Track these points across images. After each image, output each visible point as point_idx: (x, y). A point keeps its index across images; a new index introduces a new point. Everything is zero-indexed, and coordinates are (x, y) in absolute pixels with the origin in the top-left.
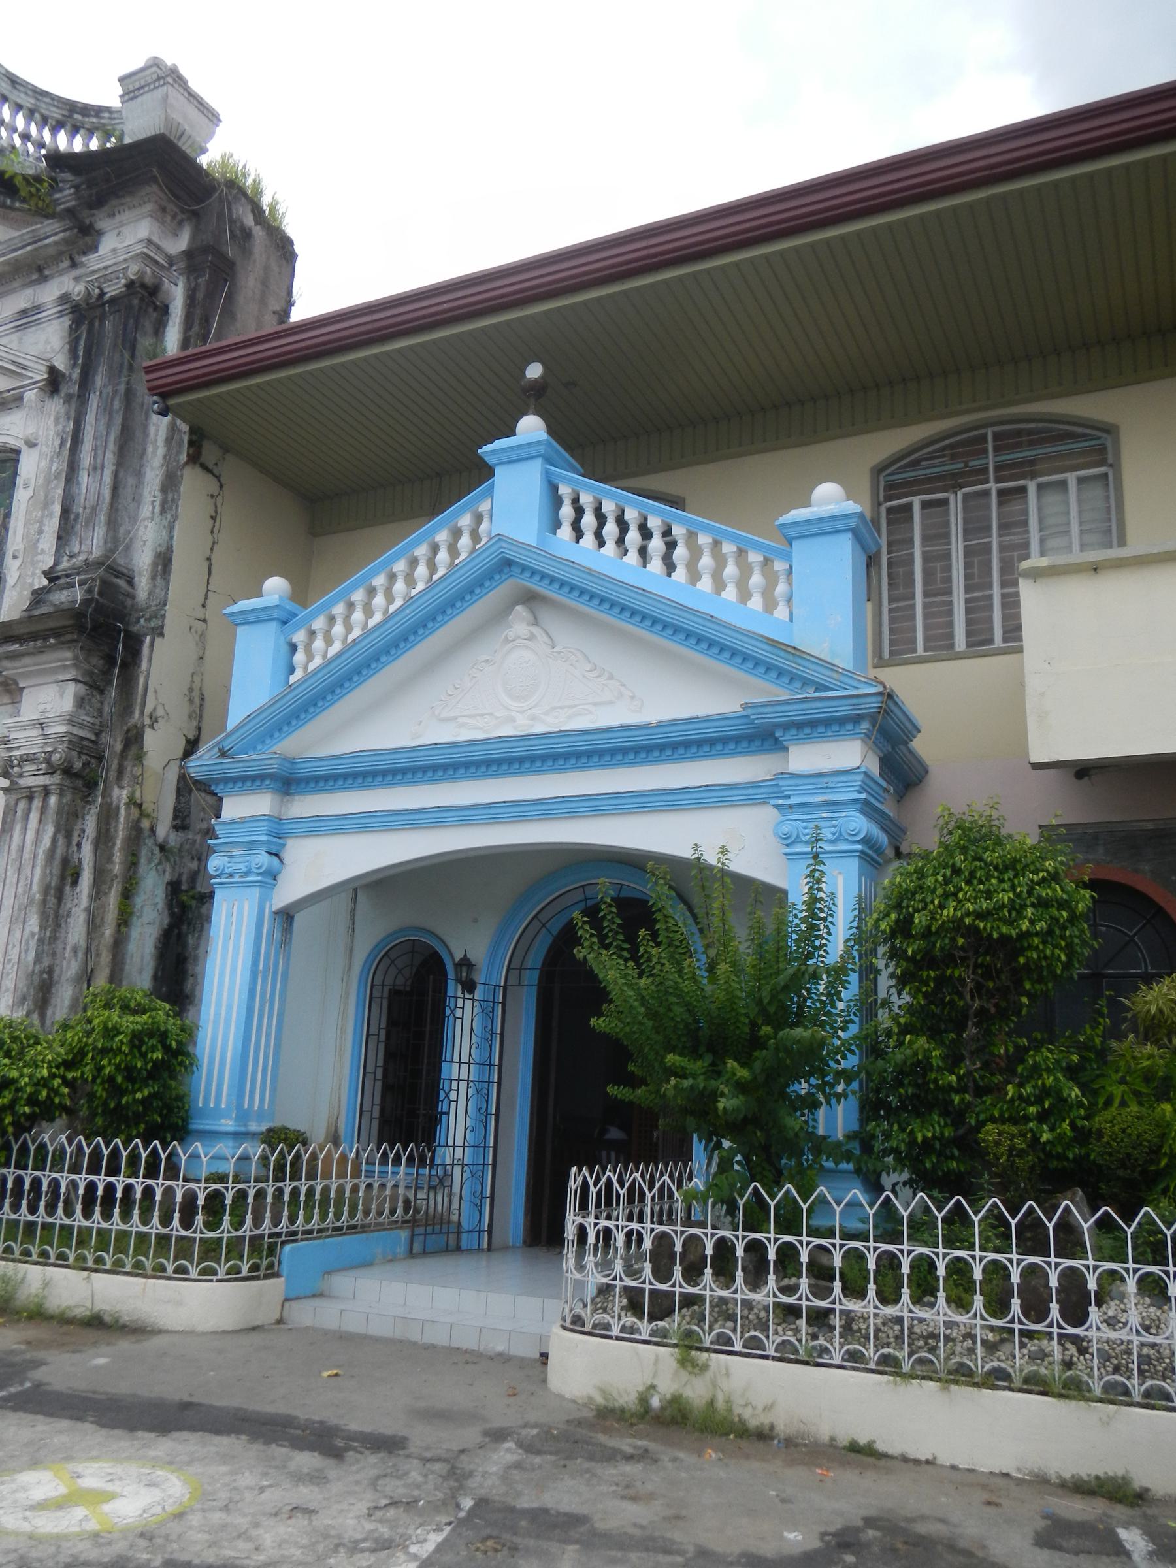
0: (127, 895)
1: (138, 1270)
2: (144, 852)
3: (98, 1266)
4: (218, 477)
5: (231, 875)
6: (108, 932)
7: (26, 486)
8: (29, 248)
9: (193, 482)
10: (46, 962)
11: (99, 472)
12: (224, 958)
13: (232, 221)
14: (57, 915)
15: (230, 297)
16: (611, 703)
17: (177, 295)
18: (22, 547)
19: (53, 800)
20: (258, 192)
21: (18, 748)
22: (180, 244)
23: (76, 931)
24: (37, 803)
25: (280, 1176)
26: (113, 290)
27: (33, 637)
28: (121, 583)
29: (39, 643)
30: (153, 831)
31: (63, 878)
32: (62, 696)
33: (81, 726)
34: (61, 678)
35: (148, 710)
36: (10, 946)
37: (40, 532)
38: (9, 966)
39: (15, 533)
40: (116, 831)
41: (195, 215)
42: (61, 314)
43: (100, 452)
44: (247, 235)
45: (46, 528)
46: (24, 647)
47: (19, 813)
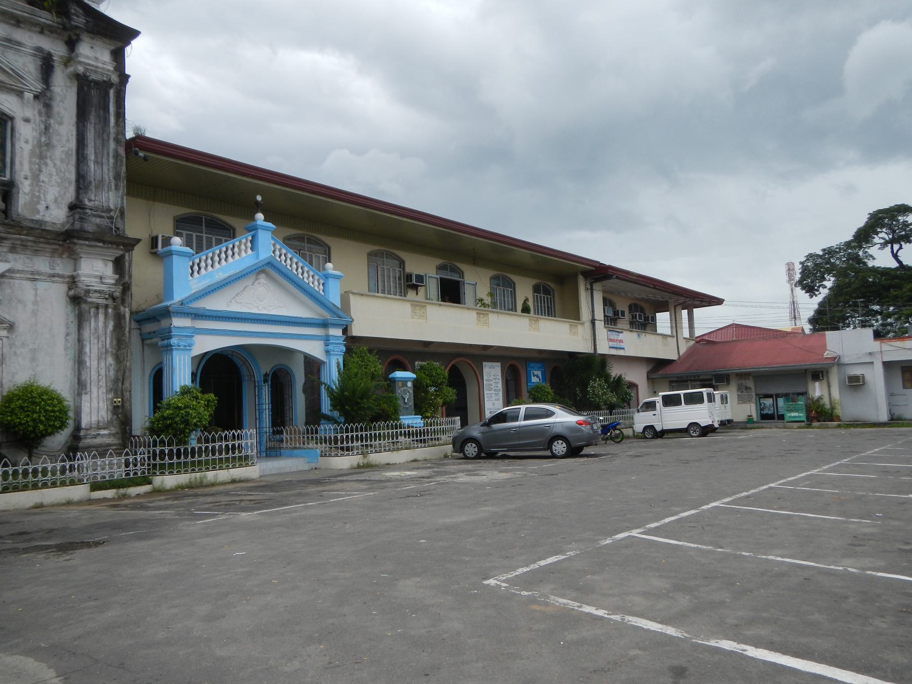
1: (241, 466)
3: (228, 467)
5: (179, 346)
7: (27, 142)
8: (26, 14)
11: (100, 165)
12: (180, 375)
16: (282, 307)
18: (29, 174)
19: (110, 310)
21: (93, 286)
24: (101, 311)
25: (308, 433)
26: (93, 77)
27: (111, 243)
29: (114, 246)
32: (106, 265)
34: (106, 258)
36: (100, 369)
37: (40, 171)
38: (100, 377)
39: (21, 164)
40: (125, 324)
42: (34, 55)
43: (99, 156)
45: (44, 170)
46: (106, 246)
47: (92, 313)
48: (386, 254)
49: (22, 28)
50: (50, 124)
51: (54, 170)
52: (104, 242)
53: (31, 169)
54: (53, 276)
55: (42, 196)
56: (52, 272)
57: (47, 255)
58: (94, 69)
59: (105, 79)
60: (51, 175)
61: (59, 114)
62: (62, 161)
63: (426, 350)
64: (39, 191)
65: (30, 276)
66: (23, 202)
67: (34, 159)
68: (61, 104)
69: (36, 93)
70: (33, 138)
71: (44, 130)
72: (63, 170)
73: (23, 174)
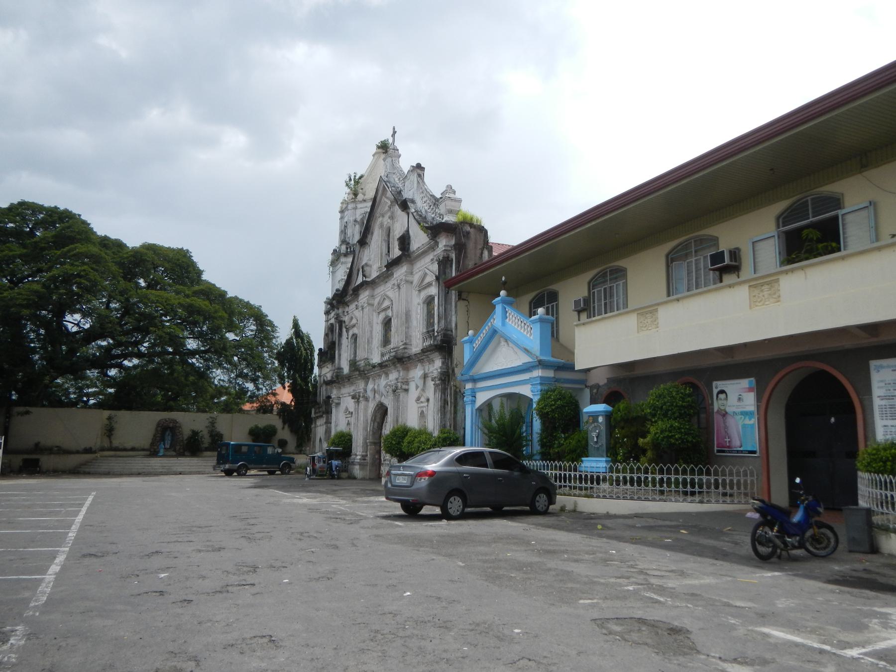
0: (455, 407)
2: (458, 396)
4: (467, 300)
6: (452, 415)
9: (462, 304)
10: (443, 423)
13: (463, 232)
14: (444, 412)
15: (465, 253)
17: (453, 256)
20: (472, 219)
22: (453, 242)
23: (448, 416)
28: (449, 333)
30: (460, 391)
31: (445, 404)
33: (443, 369)
35: (455, 363)
41: (455, 234)
44: (468, 233)
48: (695, 241)
52: (430, 351)
63: (729, 360)
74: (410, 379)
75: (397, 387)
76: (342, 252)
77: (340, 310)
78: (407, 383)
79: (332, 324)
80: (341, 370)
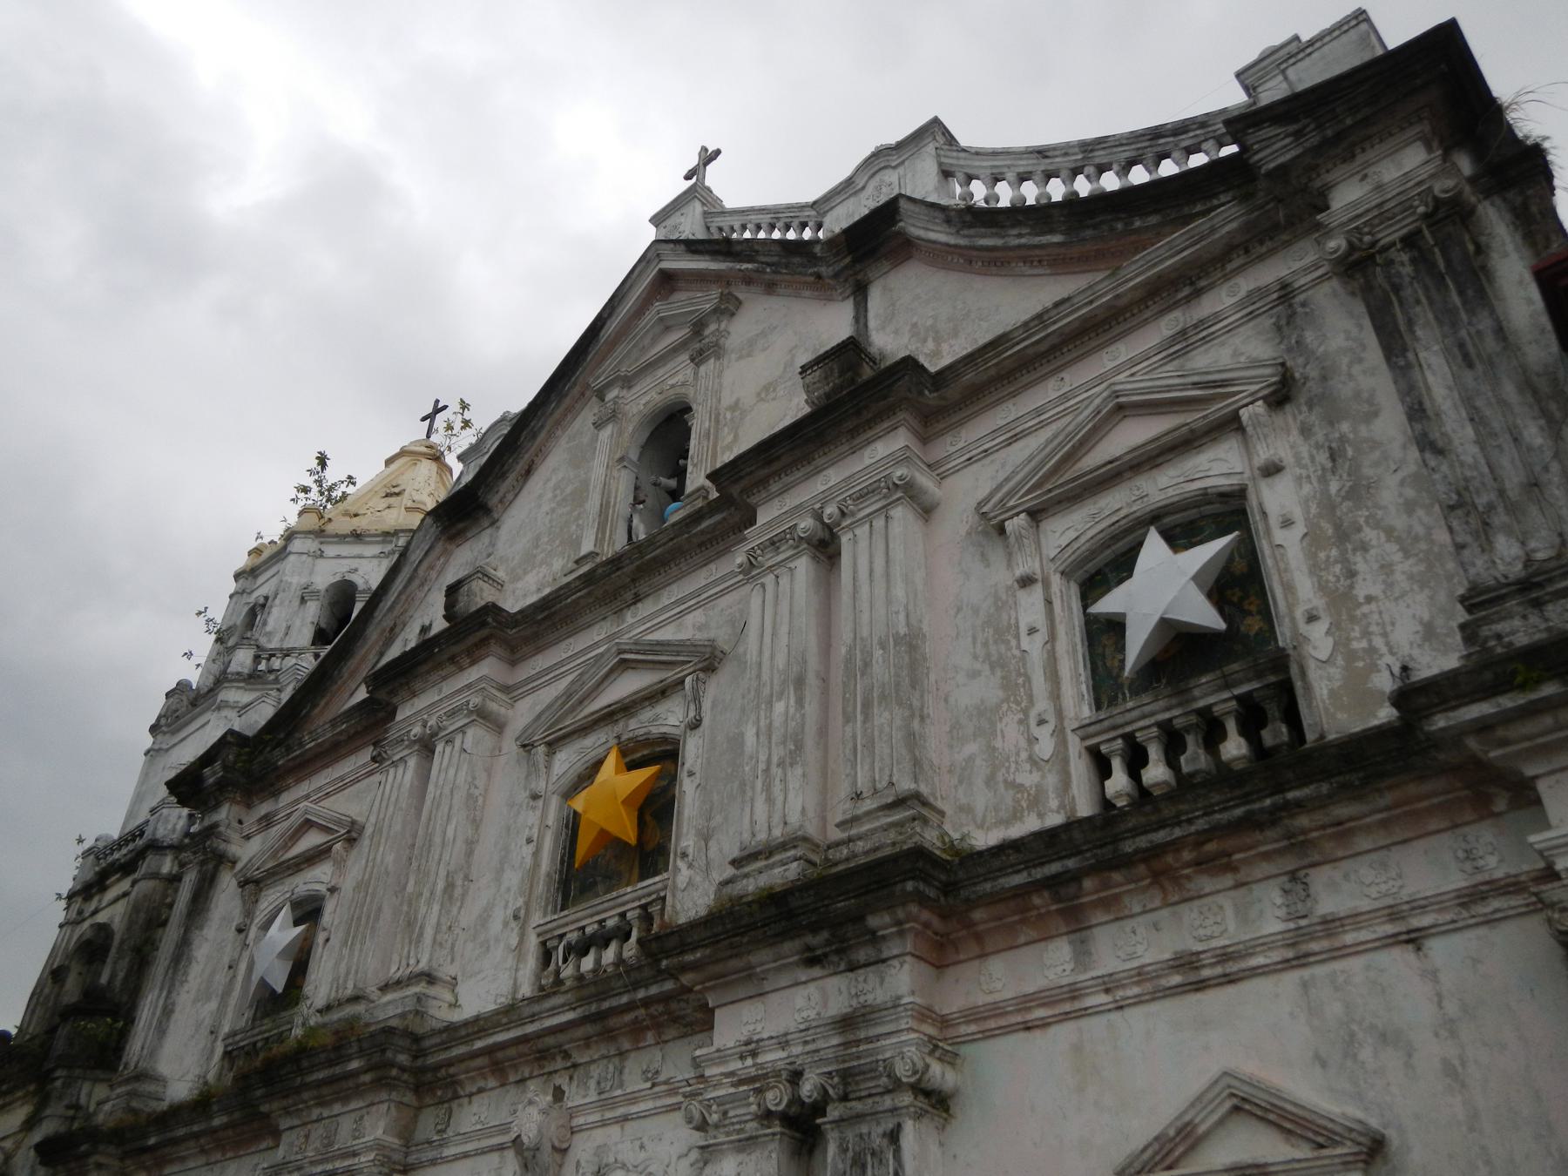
7: (1287, 523)
18: (1319, 603)
37: (1352, 574)
39: (1289, 588)
45: (1361, 566)
49: (1211, 287)
50: (1343, 439)
51: (1392, 548)
53: (1322, 587)
54: (1471, 897)
55: (1379, 642)
56: (1458, 881)
57: (1433, 826)
58: (1375, 213)
59: (1421, 209)
60: (1387, 568)
61: (1357, 395)
62: (1409, 507)
64: (1366, 634)
65: (1390, 929)
66: (1325, 692)
67: (1322, 555)
68: (1356, 369)
69: (1266, 392)
70: (1305, 503)
71: (1329, 465)
72: (1420, 530)
73: (1299, 614)
74: (973, 1015)
75: (848, 1079)
76: (233, 668)
77: (224, 814)
78: (944, 1048)
79: (104, 929)
80: (150, 1087)
